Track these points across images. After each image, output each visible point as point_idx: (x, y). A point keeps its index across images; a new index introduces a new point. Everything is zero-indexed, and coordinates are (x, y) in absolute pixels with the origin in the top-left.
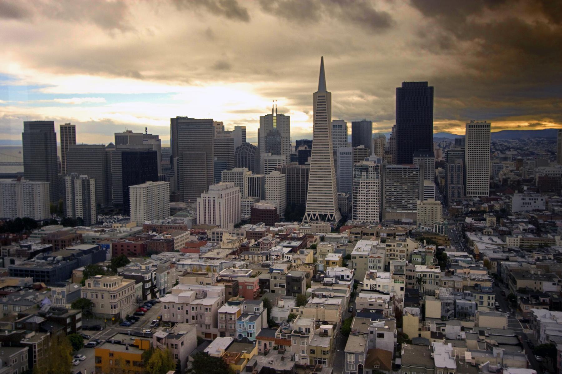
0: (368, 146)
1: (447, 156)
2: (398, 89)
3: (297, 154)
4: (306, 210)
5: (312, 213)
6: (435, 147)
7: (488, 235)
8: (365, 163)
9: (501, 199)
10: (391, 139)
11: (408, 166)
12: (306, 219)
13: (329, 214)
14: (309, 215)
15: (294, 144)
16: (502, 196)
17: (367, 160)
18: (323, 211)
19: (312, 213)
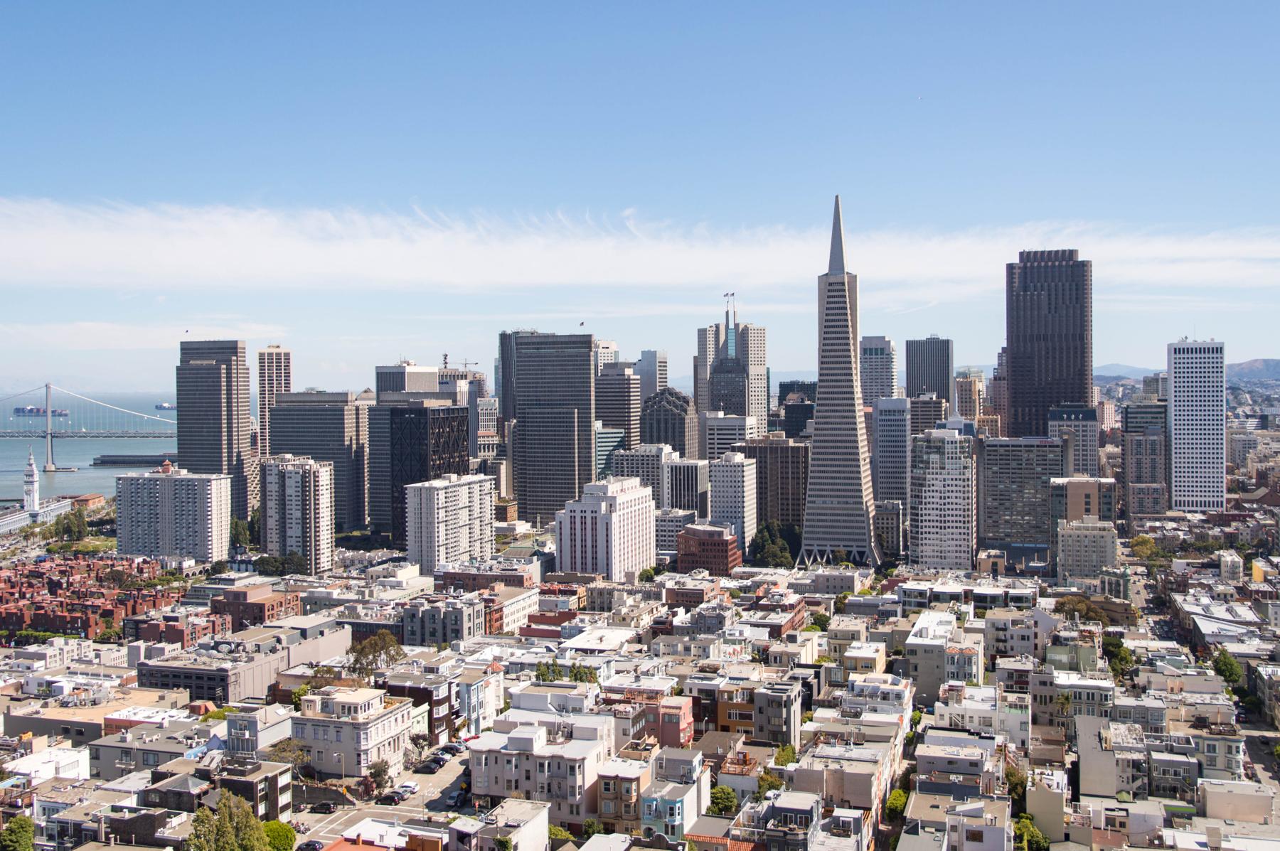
0: (944, 393)
1: (1127, 418)
2: (1010, 267)
3: (783, 413)
4: (804, 542)
5: (815, 549)
6: (1096, 396)
7: (1227, 602)
8: (936, 433)
9: (1252, 517)
10: (995, 379)
11: (1035, 441)
12: (802, 562)
13: (855, 550)
16: (1255, 510)
17: (944, 426)
18: (842, 543)
19: (815, 549)
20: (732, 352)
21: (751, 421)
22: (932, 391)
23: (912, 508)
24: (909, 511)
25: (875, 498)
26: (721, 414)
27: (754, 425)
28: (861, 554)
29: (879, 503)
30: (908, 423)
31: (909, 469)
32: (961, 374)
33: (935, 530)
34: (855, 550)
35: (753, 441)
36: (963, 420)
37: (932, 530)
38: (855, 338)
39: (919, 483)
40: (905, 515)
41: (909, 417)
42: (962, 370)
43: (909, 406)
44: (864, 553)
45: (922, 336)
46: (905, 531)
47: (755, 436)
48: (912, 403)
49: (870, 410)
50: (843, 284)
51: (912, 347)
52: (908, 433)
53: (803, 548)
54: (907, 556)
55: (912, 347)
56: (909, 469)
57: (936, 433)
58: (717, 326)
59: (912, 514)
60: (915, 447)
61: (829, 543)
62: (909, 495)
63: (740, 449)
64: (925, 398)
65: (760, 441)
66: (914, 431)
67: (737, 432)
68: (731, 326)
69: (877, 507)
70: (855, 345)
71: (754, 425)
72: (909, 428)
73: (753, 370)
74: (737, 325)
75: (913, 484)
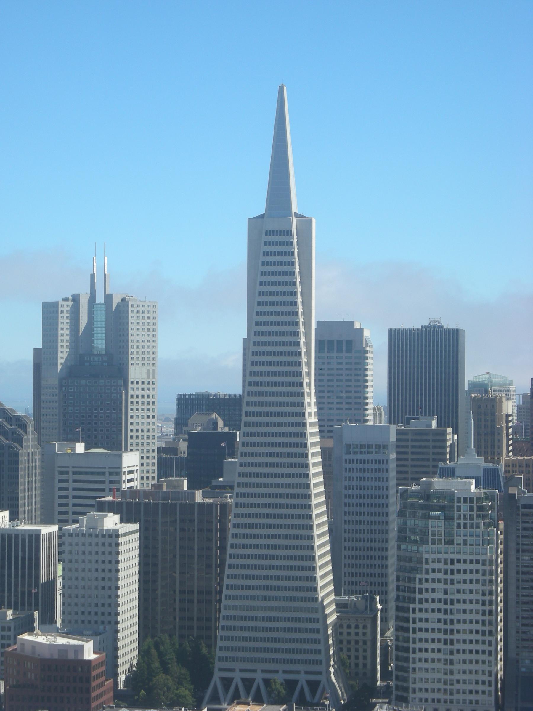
0: (450, 419)
3: (183, 446)
4: (218, 665)
5: (237, 676)
8: (439, 483)
13: (303, 678)
14: (227, 682)
15: (171, 408)
17: (450, 473)
18: (281, 667)
19: (237, 676)
20: (100, 342)
21: (130, 460)
22: (430, 414)
23: (398, 609)
24: (392, 613)
25: (337, 592)
26: (80, 448)
27: (134, 465)
28: (314, 686)
29: (344, 598)
30: (392, 466)
31: (392, 543)
32: (481, 387)
33: (436, 646)
34: (303, 678)
35: (133, 492)
36: (481, 461)
37: (431, 646)
38: (308, 324)
39: (410, 567)
40: (384, 620)
41: (393, 456)
42: (478, 380)
43: (393, 438)
44: (318, 683)
45: (414, 322)
46: (385, 648)
47: (136, 484)
48: (399, 433)
49: (330, 443)
50: (289, 233)
51: (399, 340)
52: (392, 483)
53: (217, 676)
54: (388, 687)
55: (399, 340)
56: (392, 543)
57: (439, 483)
58: (76, 299)
59: (398, 618)
60: (404, 506)
61: (260, 666)
62: (392, 587)
63: (113, 508)
64: (416, 425)
65: (146, 494)
66: (402, 479)
67: (107, 478)
68: (100, 299)
69: (341, 606)
70: (307, 334)
71: (134, 465)
72: (392, 474)
73: (135, 373)
74: (109, 298)
75: (400, 569)
